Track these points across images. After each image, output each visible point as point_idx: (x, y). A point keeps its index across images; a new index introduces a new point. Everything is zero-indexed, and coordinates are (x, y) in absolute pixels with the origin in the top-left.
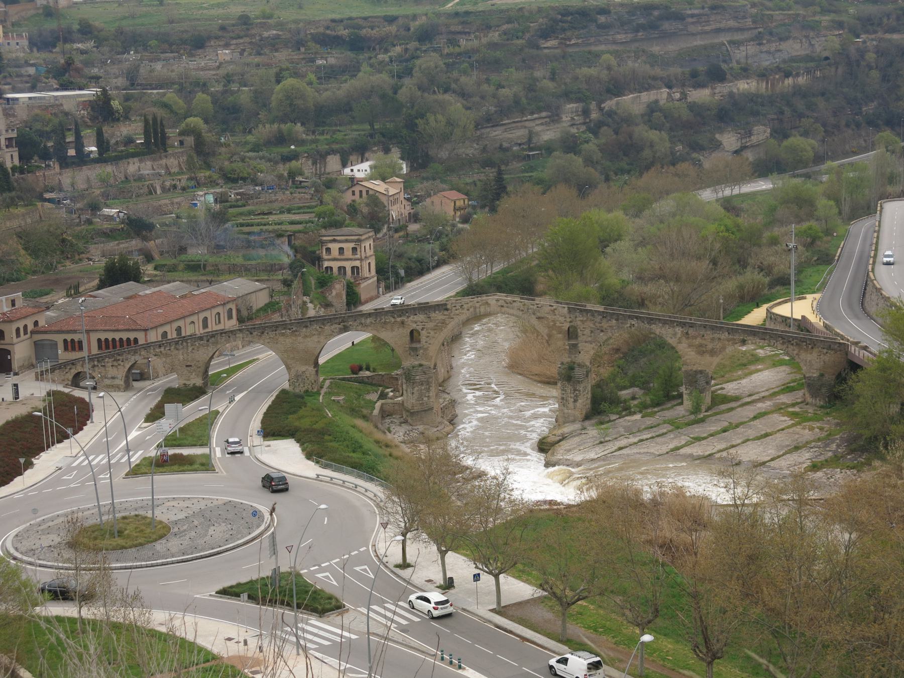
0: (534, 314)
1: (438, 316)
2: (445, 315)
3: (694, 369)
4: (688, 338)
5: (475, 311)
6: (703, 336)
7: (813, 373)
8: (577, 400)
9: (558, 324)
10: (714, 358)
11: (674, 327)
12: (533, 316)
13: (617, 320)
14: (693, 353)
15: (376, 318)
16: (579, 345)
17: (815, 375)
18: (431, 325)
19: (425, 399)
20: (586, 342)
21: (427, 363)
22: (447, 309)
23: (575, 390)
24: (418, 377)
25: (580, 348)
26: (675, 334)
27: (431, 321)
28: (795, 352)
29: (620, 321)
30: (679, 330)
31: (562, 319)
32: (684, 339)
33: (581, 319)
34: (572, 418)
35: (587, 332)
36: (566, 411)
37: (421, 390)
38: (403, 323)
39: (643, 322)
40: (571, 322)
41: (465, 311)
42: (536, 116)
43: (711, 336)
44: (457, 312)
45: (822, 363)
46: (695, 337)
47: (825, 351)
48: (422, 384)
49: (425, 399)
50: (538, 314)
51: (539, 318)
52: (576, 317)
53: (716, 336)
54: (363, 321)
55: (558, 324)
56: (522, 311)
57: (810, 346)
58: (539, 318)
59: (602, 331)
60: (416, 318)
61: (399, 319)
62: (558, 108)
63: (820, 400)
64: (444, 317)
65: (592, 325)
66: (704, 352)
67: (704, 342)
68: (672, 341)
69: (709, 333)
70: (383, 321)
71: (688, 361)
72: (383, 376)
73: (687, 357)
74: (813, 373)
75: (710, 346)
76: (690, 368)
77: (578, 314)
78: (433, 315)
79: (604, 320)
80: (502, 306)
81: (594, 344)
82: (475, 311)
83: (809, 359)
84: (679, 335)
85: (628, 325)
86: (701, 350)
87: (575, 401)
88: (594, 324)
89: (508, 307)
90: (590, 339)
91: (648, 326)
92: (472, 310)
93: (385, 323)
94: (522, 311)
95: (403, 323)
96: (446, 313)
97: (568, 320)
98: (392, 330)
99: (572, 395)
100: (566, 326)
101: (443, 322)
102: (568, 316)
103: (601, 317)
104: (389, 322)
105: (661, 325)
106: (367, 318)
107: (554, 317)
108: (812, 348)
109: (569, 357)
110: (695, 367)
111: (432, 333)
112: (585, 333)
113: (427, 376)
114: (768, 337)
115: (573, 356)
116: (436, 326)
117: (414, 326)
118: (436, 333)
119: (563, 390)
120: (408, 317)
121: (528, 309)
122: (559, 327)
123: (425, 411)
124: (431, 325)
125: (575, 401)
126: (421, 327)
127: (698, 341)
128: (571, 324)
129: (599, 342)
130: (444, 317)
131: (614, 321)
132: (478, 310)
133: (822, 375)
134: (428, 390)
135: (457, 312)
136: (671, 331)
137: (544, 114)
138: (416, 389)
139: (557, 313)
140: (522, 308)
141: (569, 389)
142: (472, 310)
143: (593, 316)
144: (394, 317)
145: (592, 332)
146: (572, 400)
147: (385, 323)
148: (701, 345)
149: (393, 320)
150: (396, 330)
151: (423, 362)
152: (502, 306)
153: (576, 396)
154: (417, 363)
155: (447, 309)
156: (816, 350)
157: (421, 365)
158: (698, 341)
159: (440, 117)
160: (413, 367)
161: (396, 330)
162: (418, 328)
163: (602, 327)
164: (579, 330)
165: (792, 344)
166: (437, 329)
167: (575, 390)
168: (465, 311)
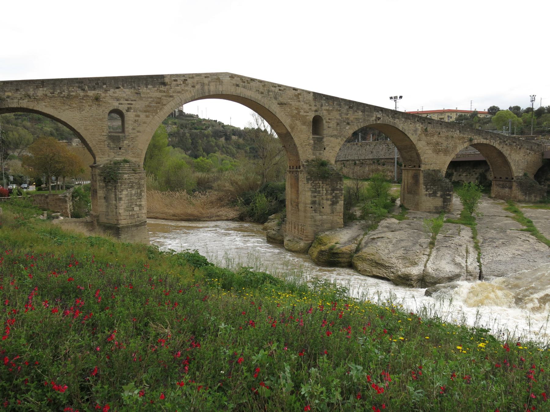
0: (276, 98)
1: (152, 92)
2: (161, 91)
3: (431, 169)
4: (426, 135)
5: (203, 89)
6: (439, 134)
7: (520, 173)
8: (337, 202)
9: (302, 113)
10: (448, 157)
11: (415, 122)
12: (274, 101)
13: (363, 111)
14: (430, 152)
15: (54, 90)
16: (325, 140)
17: (521, 175)
18: (139, 105)
19: (136, 209)
20: (332, 136)
21: (134, 160)
22: (164, 84)
23: (333, 190)
24: (126, 176)
25: (326, 143)
26: (416, 131)
27: (141, 99)
28: (508, 152)
29: (366, 113)
30: (419, 126)
31: (306, 107)
32: (423, 136)
33: (327, 108)
34: (326, 226)
35: (333, 124)
36: (318, 217)
37: (131, 194)
38: (97, 99)
39: (388, 116)
40: (316, 111)
41: (189, 88)
42: (61, 141)
43: (447, 134)
44: (179, 88)
45: (526, 163)
46: (433, 136)
47: (528, 151)
48: (132, 187)
49: (136, 209)
50: (281, 99)
51: (281, 104)
52: (322, 106)
53: (450, 134)
54: (31, 92)
55: (302, 113)
56: (262, 93)
57: (519, 147)
58: (281, 104)
59: (348, 124)
60: (118, 93)
61: (91, 93)
62: (71, 139)
63: (535, 197)
64: (158, 95)
65: (338, 117)
66: (439, 151)
67: (440, 140)
68: (413, 138)
69: (444, 130)
70: (65, 93)
71: (426, 160)
72: (47, 197)
73: (425, 156)
74: (520, 173)
75: (445, 144)
76: (428, 167)
77: (323, 102)
78: (143, 90)
79: (351, 112)
80: (237, 85)
81: (340, 139)
82: (203, 89)
83: (517, 159)
84: (419, 132)
85: (374, 118)
86: (437, 149)
87: (334, 203)
88: (340, 115)
89: (244, 87)
90: (335, 133)
91: (392, 121)
92: (198, 87)
93: (69, 97)
94: (262, 93)
95: (97, 99)
96: (163, 88)
97: (314, 108)
98: (81, 109)
99: (329, 197)
100: (311, 116)
101: (159, 101)
102: (313, 103)
103: (347, 107)
104: (76, 97)
105: (403, 120)
106: (37, 87)
107: (298, 104)
108: (520, 148)
109: (314, 154)
110: (432, 166)
111: (143, 116)
112: (331, 125)
113: (137, 176)
114: (489, 137)
115: (318, 153)
116: (149, 106)
117: (115, 105)
118: (147, 116)
119: (313, 192)
120: (106, 91)
121: (269, 91)
122: (303, 116)
123: (137, 226)
124: (139, 105)
125: (334, 203)
126: (126, 107)
127: (435, 139)
128: (317, 114)
129: (345, 137)
130: (158, 95)
131: (361, 113)
132: (206, 87)
133: (525, 175)
134: (139, 196)
135: (179, 88)
136: (412, 126)
137: (65, 141)
138: (125, 192)
139: (301, 99)
140: (261, 90)
141: (324, 189)
142: (198, 87)
143: (340, 105)
144: (83, 90)
145: (338, 124)
146: (329, 202)
147: (69, 97)
148: (437, 144)
149: (82, 94)
150: (87, 108)
151: (129, 158)
152: (237, 85)
153: (336, 197)
154: (119, 159)
155: (164, 84)
156: (522, 150)
157: (126, 161)
158: (435, 139)
159: (15, 133)
160: (115, 163)
161: (87, 108)
162: (121, 108)
163: (348, 119)
164: (324, 122)
165: (506, 144)
166: (150, 110)
167: (333, 190)
168: (189, 88)
